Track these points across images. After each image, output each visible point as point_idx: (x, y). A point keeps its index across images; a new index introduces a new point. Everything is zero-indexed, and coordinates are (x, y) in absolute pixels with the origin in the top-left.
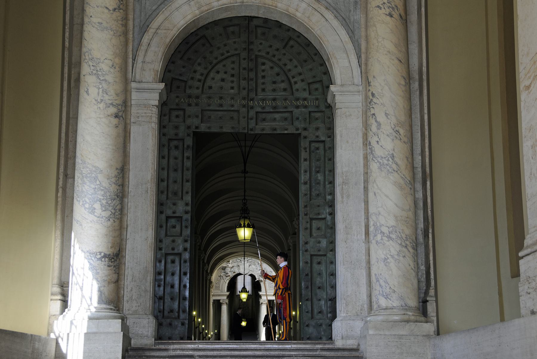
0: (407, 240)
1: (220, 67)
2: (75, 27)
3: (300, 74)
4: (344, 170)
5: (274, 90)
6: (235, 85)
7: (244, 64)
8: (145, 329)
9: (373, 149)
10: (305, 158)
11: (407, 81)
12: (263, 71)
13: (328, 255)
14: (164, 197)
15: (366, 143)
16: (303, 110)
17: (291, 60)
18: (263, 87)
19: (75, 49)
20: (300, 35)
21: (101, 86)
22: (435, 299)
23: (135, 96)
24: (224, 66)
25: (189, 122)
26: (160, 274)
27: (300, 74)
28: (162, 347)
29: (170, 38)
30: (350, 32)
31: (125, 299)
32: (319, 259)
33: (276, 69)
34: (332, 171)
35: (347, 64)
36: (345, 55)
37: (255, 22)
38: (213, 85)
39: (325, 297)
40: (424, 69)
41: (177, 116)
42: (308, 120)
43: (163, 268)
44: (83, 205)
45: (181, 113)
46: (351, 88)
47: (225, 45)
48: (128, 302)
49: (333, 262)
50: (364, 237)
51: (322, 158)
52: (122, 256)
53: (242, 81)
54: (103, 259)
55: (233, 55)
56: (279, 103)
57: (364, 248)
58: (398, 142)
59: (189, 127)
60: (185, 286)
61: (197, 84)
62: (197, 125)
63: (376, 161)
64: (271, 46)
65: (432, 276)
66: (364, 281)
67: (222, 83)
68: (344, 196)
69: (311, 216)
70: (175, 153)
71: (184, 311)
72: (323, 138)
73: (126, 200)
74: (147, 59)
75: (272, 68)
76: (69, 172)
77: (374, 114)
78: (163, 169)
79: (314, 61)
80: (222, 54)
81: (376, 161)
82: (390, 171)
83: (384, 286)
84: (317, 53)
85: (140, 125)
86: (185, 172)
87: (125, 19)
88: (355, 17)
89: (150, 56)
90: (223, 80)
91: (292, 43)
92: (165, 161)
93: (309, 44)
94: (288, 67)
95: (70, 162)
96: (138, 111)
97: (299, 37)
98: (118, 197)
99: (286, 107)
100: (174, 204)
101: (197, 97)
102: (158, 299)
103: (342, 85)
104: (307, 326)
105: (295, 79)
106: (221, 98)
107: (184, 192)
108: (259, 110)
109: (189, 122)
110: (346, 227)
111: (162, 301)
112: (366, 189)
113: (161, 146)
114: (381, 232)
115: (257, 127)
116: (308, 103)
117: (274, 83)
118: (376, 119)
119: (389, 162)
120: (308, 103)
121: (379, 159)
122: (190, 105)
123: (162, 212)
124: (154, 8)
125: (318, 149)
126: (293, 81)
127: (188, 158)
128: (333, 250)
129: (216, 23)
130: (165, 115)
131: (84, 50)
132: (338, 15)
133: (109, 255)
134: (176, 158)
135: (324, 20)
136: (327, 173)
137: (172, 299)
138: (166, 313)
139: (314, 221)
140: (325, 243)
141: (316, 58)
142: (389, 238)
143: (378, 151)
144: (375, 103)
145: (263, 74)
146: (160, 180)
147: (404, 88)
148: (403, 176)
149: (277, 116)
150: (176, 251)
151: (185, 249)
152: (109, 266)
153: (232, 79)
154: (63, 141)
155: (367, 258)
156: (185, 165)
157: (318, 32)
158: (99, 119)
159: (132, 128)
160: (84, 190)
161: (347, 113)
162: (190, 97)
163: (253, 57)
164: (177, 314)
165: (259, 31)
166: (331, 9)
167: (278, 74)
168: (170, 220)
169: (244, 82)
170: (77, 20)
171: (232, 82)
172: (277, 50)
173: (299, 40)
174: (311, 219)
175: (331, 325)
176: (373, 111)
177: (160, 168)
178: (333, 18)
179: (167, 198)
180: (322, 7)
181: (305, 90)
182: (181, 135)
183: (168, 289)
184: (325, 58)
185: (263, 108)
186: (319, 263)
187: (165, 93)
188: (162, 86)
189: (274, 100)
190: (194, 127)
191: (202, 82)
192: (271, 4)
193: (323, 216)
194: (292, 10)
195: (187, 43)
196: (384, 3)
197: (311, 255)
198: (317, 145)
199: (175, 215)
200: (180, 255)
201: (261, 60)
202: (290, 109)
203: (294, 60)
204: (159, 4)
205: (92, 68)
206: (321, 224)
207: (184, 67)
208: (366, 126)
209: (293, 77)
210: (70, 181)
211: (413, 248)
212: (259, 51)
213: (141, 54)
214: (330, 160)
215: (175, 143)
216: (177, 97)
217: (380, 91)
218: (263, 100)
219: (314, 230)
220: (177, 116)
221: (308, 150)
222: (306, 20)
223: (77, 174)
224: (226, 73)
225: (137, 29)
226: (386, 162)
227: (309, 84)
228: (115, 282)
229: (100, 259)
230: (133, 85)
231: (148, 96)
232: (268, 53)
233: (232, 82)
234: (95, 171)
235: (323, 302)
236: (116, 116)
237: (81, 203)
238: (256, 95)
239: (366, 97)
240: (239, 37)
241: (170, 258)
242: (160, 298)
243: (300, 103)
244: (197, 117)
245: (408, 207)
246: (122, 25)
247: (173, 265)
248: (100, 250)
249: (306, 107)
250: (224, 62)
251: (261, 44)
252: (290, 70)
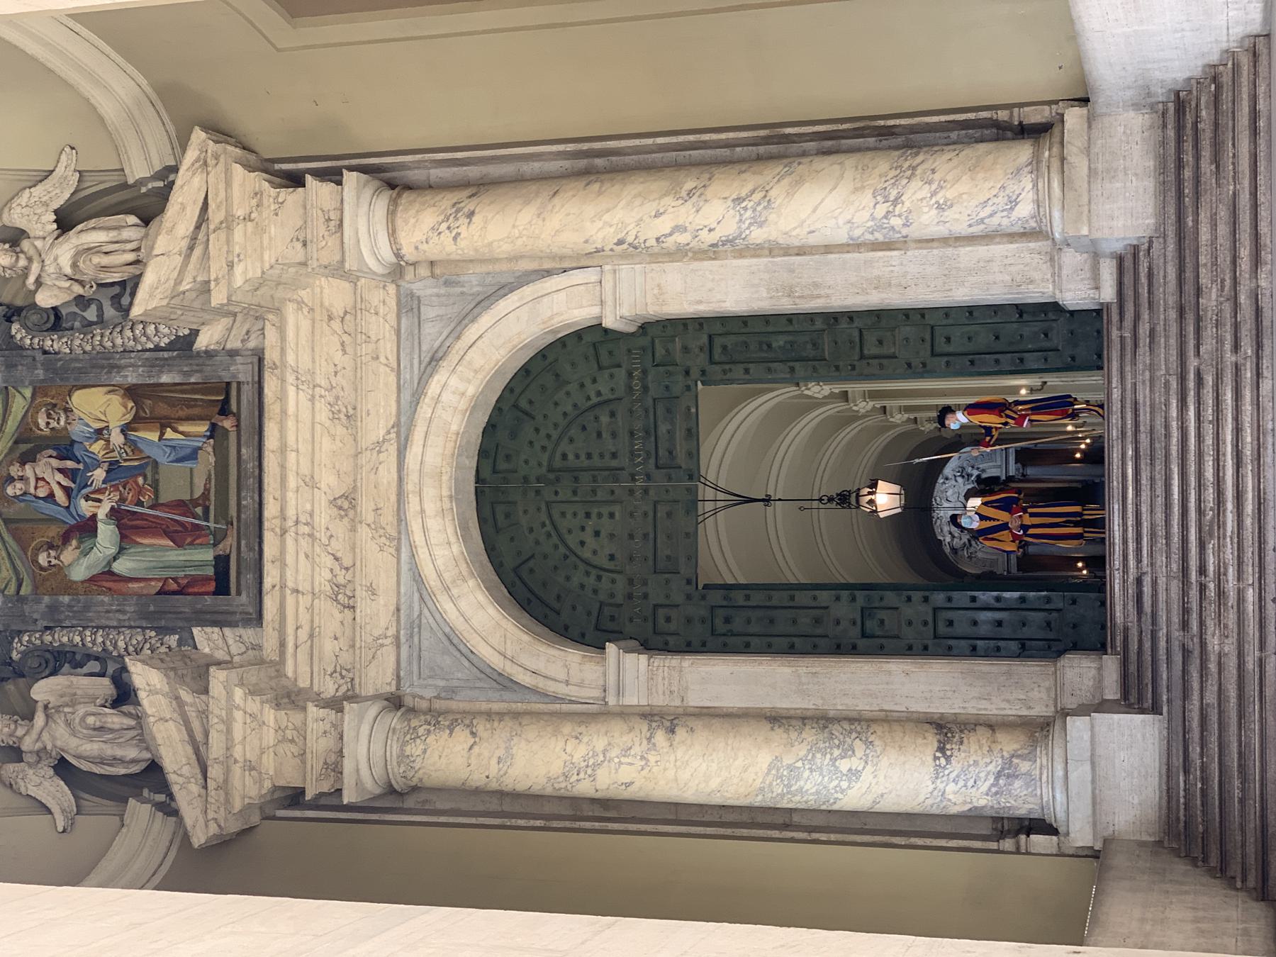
1: (572, 541)
2: (507, 807)
3: (582, 385)
4: (765, 295)
5: (614, 435)
6: (605, 511)
7: (565, 494)
8: (1083, 673)
10: (742, 371)
11: (592, 178)
12: (577, 457)
13: (932, 323)
14: (822, 642)
15: (713, 252)
16: (650, 378)
17: (556, 404)
18: (607, 456)
19: (548, 808)
20: (509, 389)
21: (616, 760)
22: (1016, 110)
23: (631, 699)
24: (570, 531)
25: (678, 598)
26: (974, 648)
27: (582, 385)
28: (1119, 640)
29: (521, 634)
30: (502, 292)
31: (1024, 712)
32: (940, 341)
33: (573, 432)
34: (766, 319)
35: (562, 295)
36: (545, 299)
37: (486, 474)
38: (607, 551)
39: (1015, 325)
40: (570, 147)
41: (668, 620)
42: (670, 368)
43: (963, 642)
44: (842, 791)
45: (661, 613)
46: (608, 285)
47: (531, 530)
48: (1030, 708)
49: (947, 311)
50: (895, 253)
51: (743, 338)
52: (941, 719)
53: (598, 498)
54: (948, 753)
55: (550, 516)
56: (638, 425)
57: (917, 252)
58: (709, 192)
59: (689, 597)
60: (998, 599)
61: (605, 584)
62: (684, 582)
64: (531, 443)
65: (971, 116)
66: (982, 251)
67: (603, 534)
68: (815, 293)
69: (856, 358)
70: (738, 624)
71: (1049, 600)
72: (705, 339)
73: (831, 714)
74: (562, 675)
75: (571, 440)
76: (780, 820)
77: (657, 239)
78: (770, 646)
79: (556, 360)
80: (549, 535)
84: (542, 354)
85: (687, 688)
86: (774, 602)
87: (489, 715)
88: (475, 283)
89: (557, 671)
90: (597, 534)
91: (523, 404)
92: (755, 641)
93: (525, 372)
94: (569, 408)
95: (760, 819)
96: (660, 692)
97: (512, 391)
98: (826, 727)
99: (646, 411)
100: (838, 623)
101: (631, 582)
102: (1025, 650)
103: (602, 303)
104: (1073, 358)
105: (593, 395)
106: (631, 537)
107: (813, 604)
108: (652, 461)
109: (678, 598)
110: (876, 288)
111: (1028, 643)
112: (801, 251)
113: (725, 649)
114: (885, 217)
115: (684, 466)
116: (636, 369)
117: (599, 435)
118: (665, 236)
120: (636, 369)
121: (744, 226)
122: (645, 596)
123: (854, 647)
124: (466, 663)
125: (724, 348)
126: (595, 400)
127: (747, 598)
128: (922, 312)
129: (490, 549)
130: (666, 643)
131: (549, 791)
132: (470, 317)
133: (939, 741)
134: (749, 622)
135: (479, 342)
136: (770, 329)
137: (1024, 625)
138: (1051, 635)
139: (866, 352)
140: (908, 328)
141: (550, 359)
142: (896, 202)
143: (729, 228)
144: (636, 237)
145: (583, 457)
146: (791, 650)
147: (607, 185)
149: (663, 428)
150: (930, 620)
151: (926, 599)
152: (962, 743)
153: (594, 516)
154: (721, 831)
155: (935, 244)
156: (761, 604)
157: (503, 352)
158: (678, 763)
159: (692, 704)
160: (814, 790)
161: (656, 291)
162: (630, 596)
163: (551, 476)
164: (1055, 614)
165: (502, 465)
166: (459, 329)
167: (584, 428)
168: (868, 631)
169: (599, 493)
170: (494, 806)
171: (600, 515)
172: (537, 430)
173: (518, 391)
174: (862, 357)
175: (1072, 313)
176: (652, 242)
177: (768, 649)
178: (476, 325)
179: (826, 636)
180: (457, 347)
181: (612, 376)
182: (704, 612)
183: (1006, 631)
184: (551, 339)
185: (648, 453)
186: (948, 340)
187: (623, 643)
188: (611, 648)
189: (632, 434)
190: (688, 587)
191: (602, 573)
192: (452, 444)
193: (856, 334)
194: (463, 404)
195: (529, 601)
196: (449, 228)
197: (933, 354)
198: (717, 351)
199: (859, 622)
200: (936, 610)
201: (558, 463)
202: (650, 401)
203: (556, 398)
204: (459, 655)
205: (582, 775)
206: (870, 338)
207: (574, 608)
208: (680, 253)
209: (589, 398)
210: (796, 818)
211: (917, 154)
212: (540, 465)
213: (552, 687)
214: (745, 323)
215: (719, 622)
216: (631, 620)
217: (612, 230)
218: (633, 454)
219: (885, 350)
220: (668, 620)
221: (727, 367)
222: (480, 377)
223: (784, 804)
224: (583, 529)
225: (507, 695)
226: (749, 213)
227: (600, 368)
228: (993, 730)
229: (948, 759)
230: (612, 700)
231: (633, 673)
232: (544, 448)
233: (600, 515)
234: (778, 770)
235: (1027, 331)
236: (672, 731)
237: (840, 796)
238: (623, 469)
239: (624, 256)
240: (514, 503)
241: (942, 629)
242: (1023, 647)
243: (636, 385)
244: (667, 581)
245: (837, 167)
246: (500, 721)
247: (955, 624)
248: (930, 759)
249: (644, 372)
250: (564, 531)
251: (526, 462)
252: (575, 406)
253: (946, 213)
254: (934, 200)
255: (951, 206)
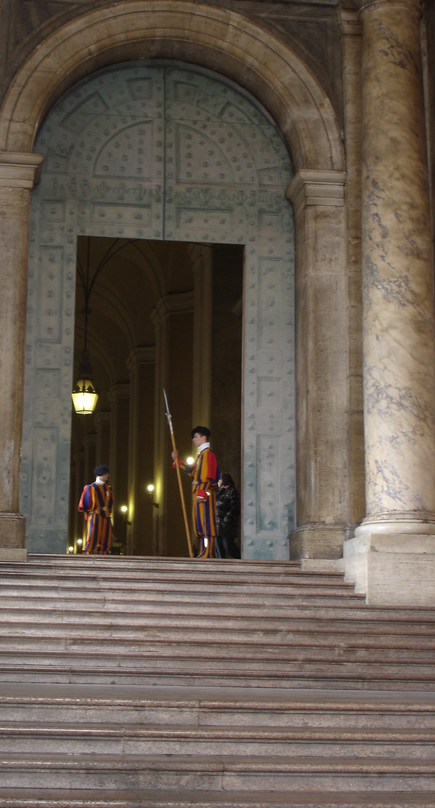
0: (426, 410)
9: (375, 267)
63: (380, 287)
77: (377, 215)
81: (380, 287)
82: (403, 302)
83: (391, 480)
114: (388, 396)
118: (379, 221)
119: (401, 289)
148: (421, 312)
253: (388, 443)
254: (400, 434)
255: (395, 448)
